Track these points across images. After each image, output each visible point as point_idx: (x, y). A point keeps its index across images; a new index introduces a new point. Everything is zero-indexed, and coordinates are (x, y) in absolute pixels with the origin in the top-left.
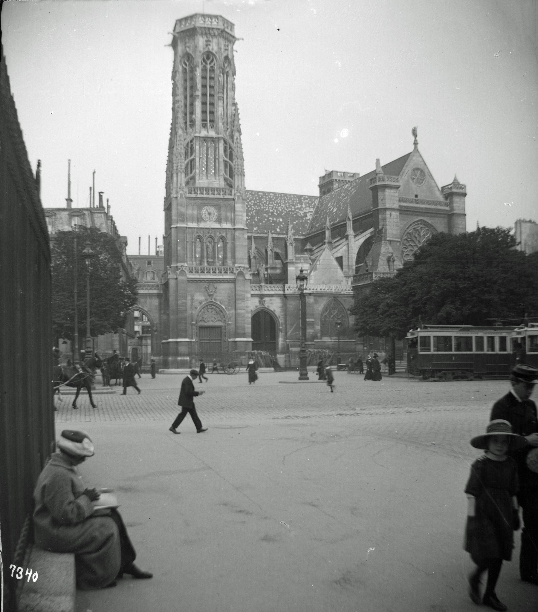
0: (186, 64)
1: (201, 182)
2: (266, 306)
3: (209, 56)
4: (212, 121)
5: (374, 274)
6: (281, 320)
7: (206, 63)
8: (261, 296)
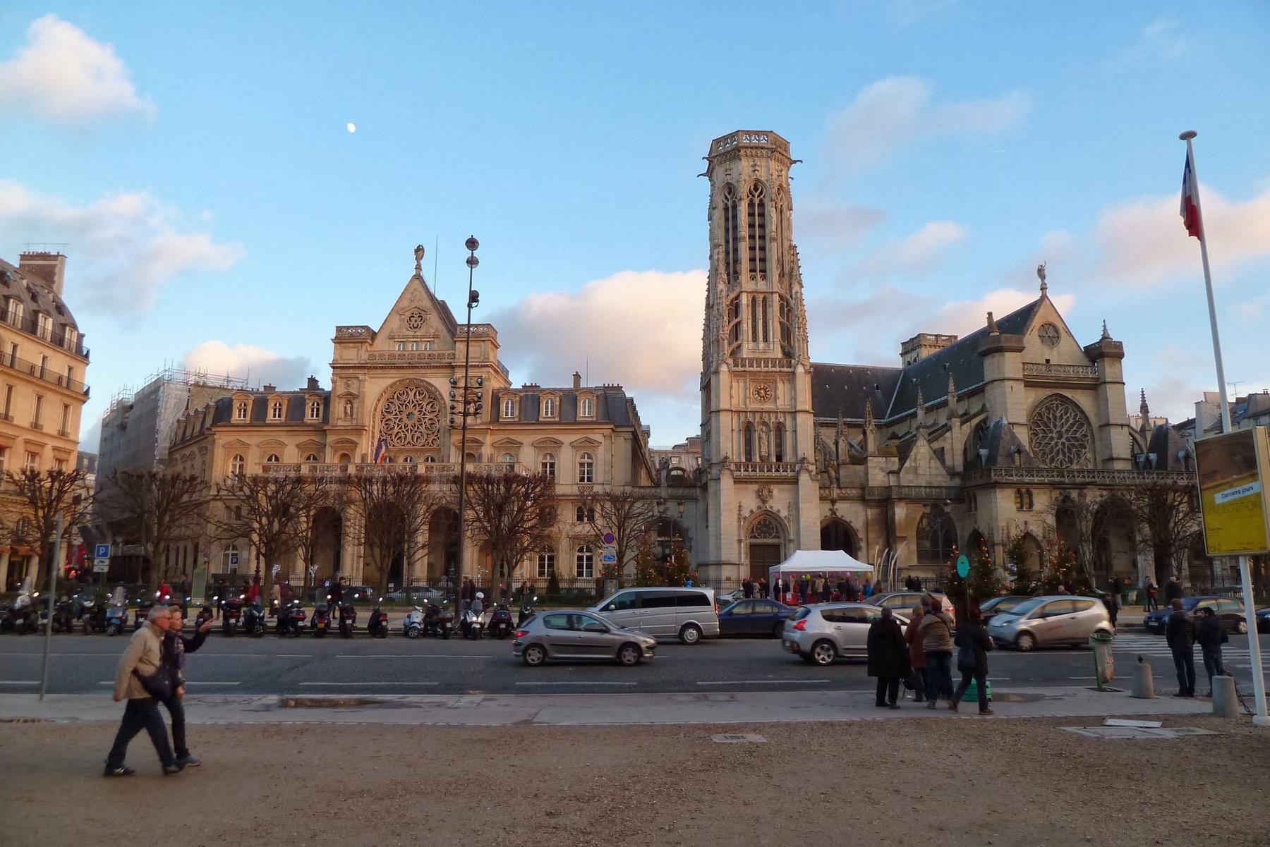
0: (726, 198)
2: (839, 514)
3: (757, 186)
4: (763, 271)
5: (993, 471)
6: (861, 535)
7: (753, 196)
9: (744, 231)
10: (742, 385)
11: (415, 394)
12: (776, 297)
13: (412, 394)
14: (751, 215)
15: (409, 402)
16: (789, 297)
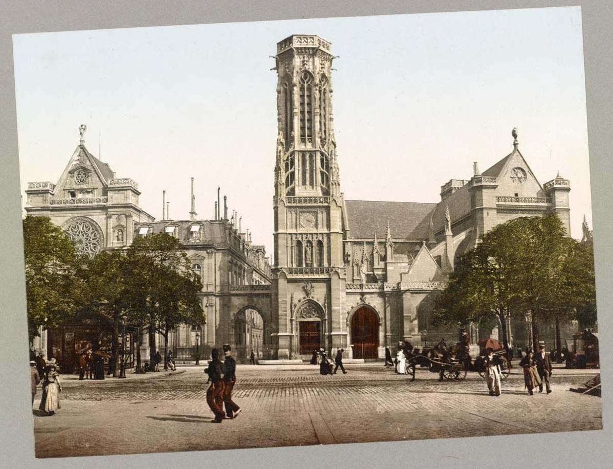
0: (286, 85)
1: (300, 191)
7: (304, 83)
8: (362, 294)
9: (297, 110)
10: (294, 215)
11: (83, 227)
12: (319, 155)
13: (81, 227)
14: (302, 96)
15: (79, 233)
16: (327, 154)
